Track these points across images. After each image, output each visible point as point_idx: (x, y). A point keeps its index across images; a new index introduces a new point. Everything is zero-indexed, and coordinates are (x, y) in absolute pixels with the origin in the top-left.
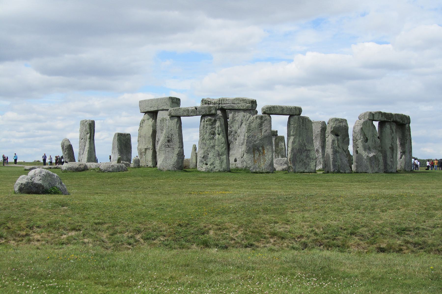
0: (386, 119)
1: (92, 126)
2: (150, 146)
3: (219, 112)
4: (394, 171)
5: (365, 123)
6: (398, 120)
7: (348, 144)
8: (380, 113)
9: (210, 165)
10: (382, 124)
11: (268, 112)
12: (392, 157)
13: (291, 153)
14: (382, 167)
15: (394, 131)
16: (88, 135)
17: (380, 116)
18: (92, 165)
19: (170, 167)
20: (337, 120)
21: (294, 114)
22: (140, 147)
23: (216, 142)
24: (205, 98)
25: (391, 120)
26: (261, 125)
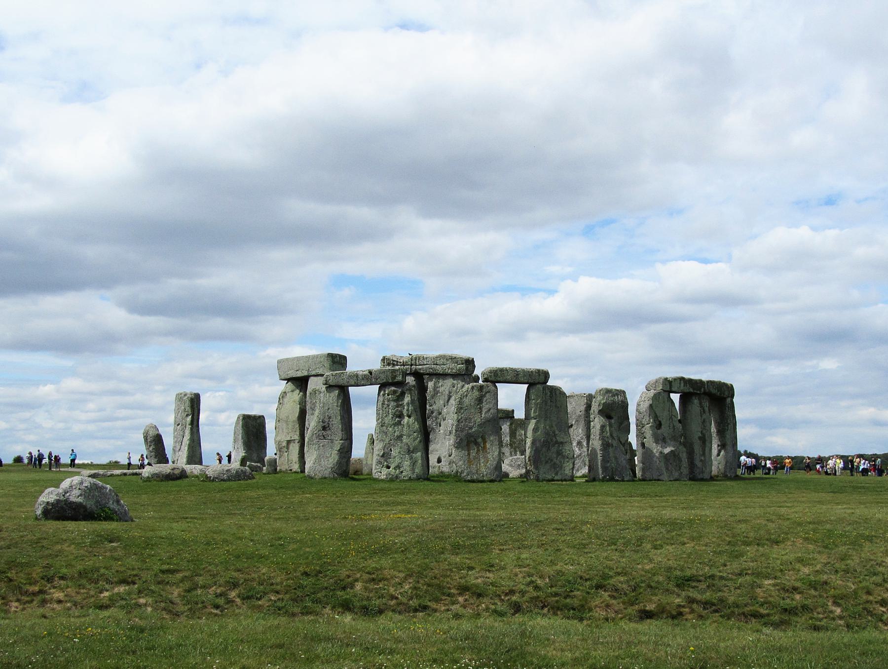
0: (691, 390)
1: (195, 402)
2: (296, 437)
3: (410, 380)
4: (706, 476)
5: (656, 397)
6: (714, 391)
7: (628, 431)
8: (682, 379)
9: (395, 469)
10: (685, 399)
11: (493, 379)
12: (704, 454)
13: (532, 447)
14: (685, 471)
15: (707, 409)
16: (189, 418)
17: (682, 385)
18: (195, 469)
19: (327, 473)
20: (608, 391)
21: (536, 381)
22: (279, 438)
23: (405, 429)
24: (388, 355)
25: (700, 390)
26: (480, 400)
